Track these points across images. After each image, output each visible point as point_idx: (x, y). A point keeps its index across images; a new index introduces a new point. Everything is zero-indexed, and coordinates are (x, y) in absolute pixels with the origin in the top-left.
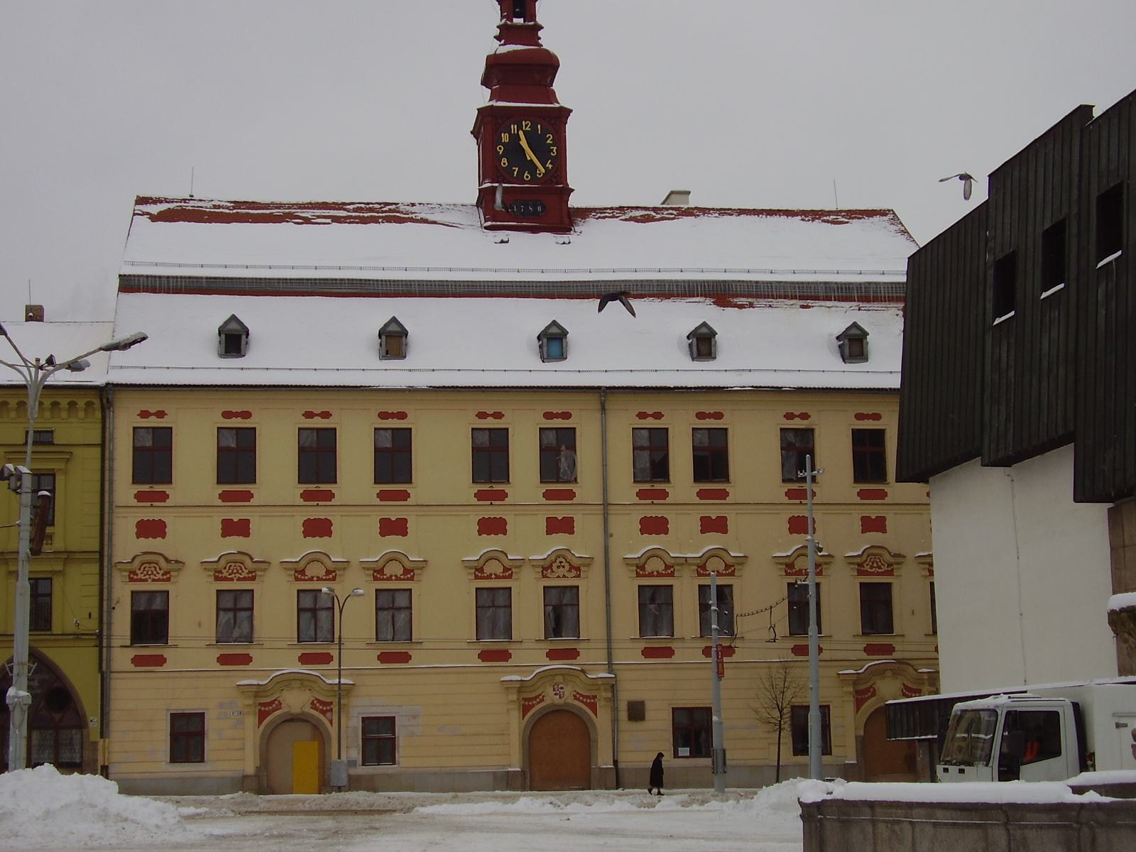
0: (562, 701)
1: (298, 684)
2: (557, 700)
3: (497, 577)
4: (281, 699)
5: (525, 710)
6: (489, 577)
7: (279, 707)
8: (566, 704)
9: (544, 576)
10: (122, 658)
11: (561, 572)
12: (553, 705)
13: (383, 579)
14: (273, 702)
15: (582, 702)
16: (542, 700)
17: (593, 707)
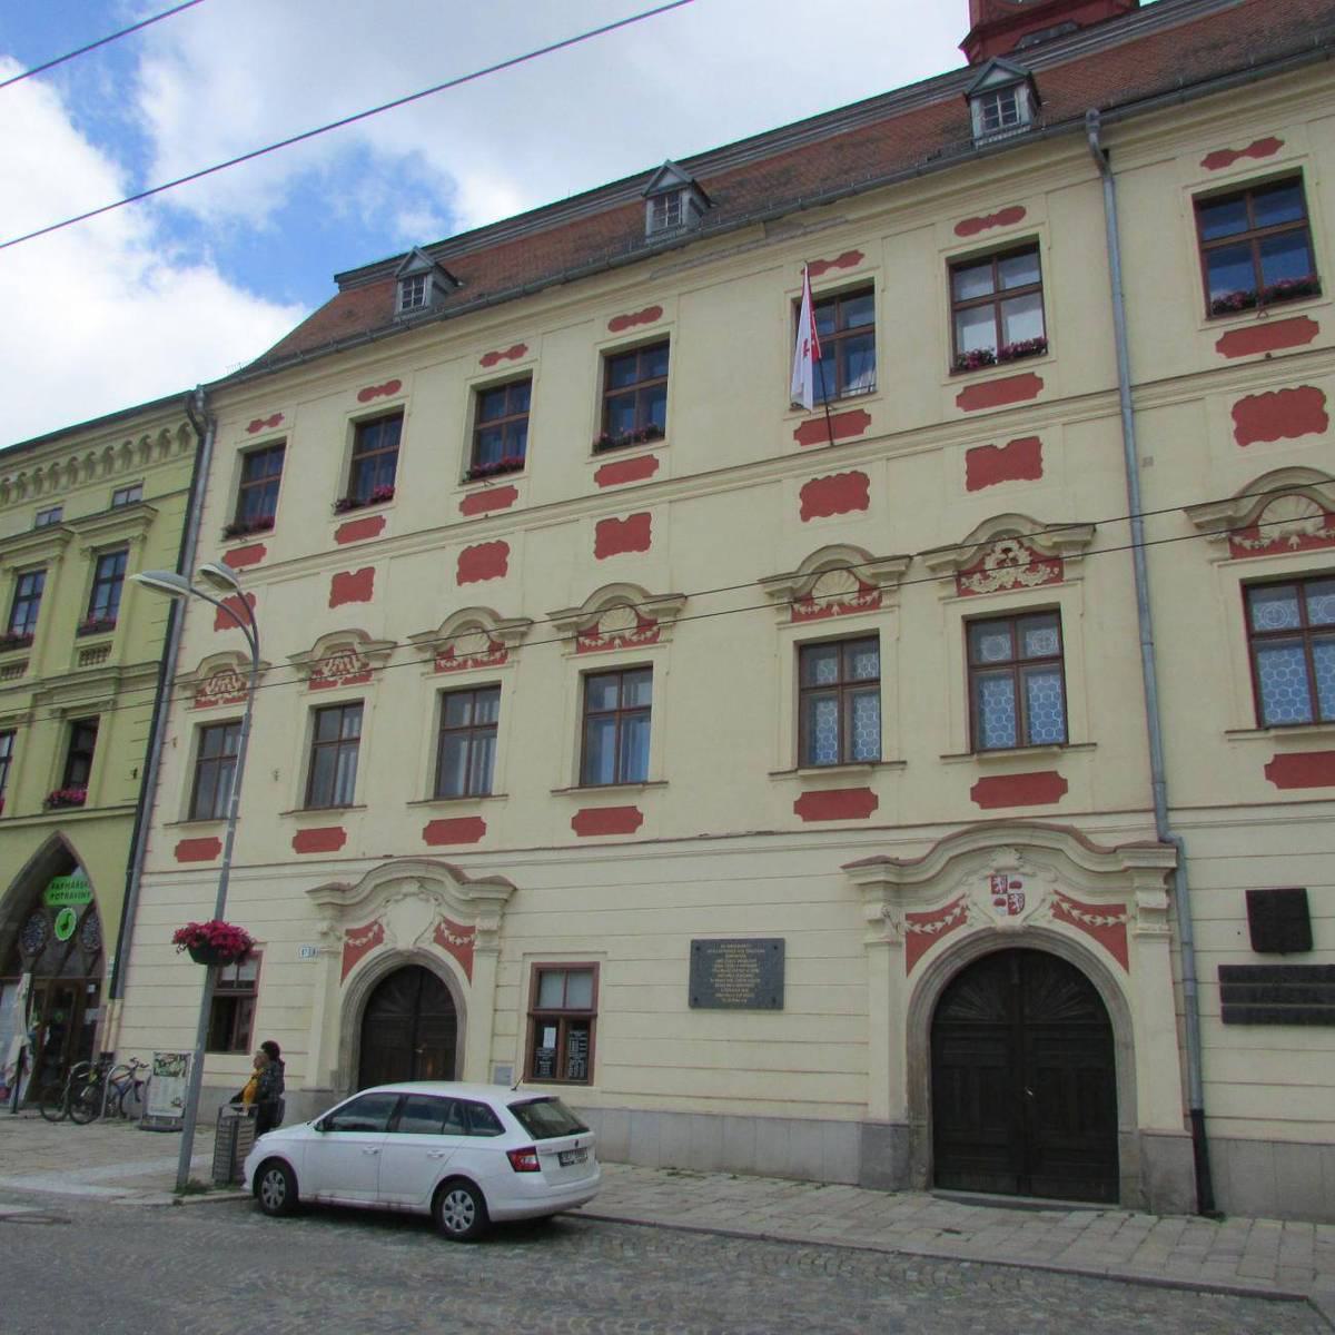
0: (1017, 922)
1: (413, 887)
2: (1003, 920)
3: (846, 609)
4: (383, 922)
5: (916, 946)
6: (826, 612)
7: (378, 939)
8: (1031, 932)
9: (964, 592)
10: (162, 844)
11: (1007, 575)
12: (992, 933)
13: (597, 648)
14: (368, 928)
15: (1080, 924)
16: (960, 920)
17: (1116, 941)
